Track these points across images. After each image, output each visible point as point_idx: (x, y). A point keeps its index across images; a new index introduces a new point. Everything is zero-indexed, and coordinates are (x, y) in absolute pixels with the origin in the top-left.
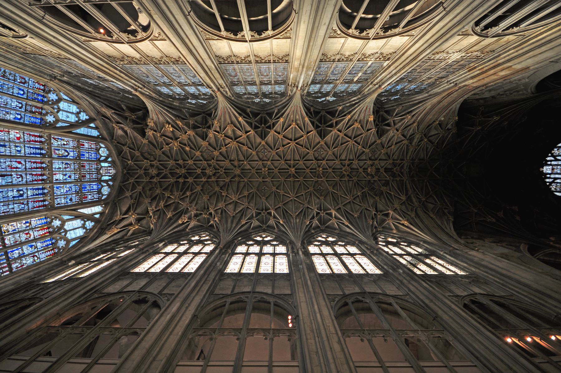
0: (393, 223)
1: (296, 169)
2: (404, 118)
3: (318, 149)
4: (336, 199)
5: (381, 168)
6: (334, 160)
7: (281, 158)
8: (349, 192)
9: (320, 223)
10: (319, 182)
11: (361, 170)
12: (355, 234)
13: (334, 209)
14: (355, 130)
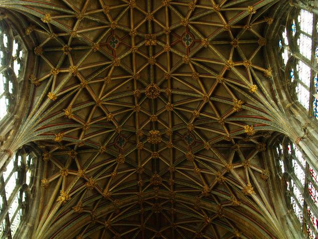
0: (58, 179)
3: (193, 35)
4: (96, 75)
5: (159, 153)
6: (171, 67)
11: (154, 117)
14: (227, 102)
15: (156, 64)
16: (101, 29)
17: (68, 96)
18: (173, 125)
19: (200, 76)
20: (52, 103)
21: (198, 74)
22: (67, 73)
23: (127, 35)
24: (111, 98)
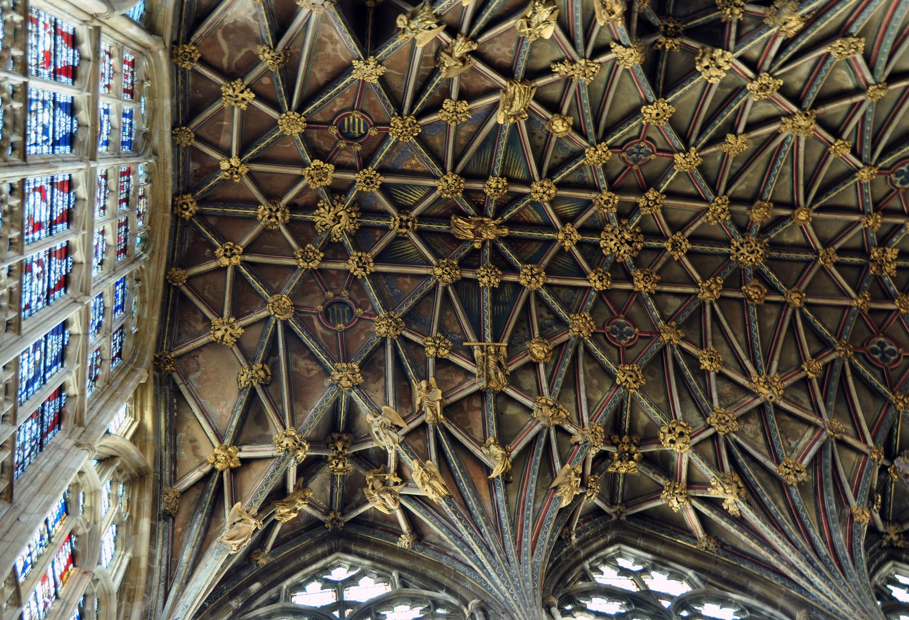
4: (700, 393)
7: (441, 163)
8: (761, 362)
9: (612, 503)
10: (621, 299)
11: (828, 259)
15: (688, 233)
16: (583, 361)
22: (690, 463)
24: (759, 353)
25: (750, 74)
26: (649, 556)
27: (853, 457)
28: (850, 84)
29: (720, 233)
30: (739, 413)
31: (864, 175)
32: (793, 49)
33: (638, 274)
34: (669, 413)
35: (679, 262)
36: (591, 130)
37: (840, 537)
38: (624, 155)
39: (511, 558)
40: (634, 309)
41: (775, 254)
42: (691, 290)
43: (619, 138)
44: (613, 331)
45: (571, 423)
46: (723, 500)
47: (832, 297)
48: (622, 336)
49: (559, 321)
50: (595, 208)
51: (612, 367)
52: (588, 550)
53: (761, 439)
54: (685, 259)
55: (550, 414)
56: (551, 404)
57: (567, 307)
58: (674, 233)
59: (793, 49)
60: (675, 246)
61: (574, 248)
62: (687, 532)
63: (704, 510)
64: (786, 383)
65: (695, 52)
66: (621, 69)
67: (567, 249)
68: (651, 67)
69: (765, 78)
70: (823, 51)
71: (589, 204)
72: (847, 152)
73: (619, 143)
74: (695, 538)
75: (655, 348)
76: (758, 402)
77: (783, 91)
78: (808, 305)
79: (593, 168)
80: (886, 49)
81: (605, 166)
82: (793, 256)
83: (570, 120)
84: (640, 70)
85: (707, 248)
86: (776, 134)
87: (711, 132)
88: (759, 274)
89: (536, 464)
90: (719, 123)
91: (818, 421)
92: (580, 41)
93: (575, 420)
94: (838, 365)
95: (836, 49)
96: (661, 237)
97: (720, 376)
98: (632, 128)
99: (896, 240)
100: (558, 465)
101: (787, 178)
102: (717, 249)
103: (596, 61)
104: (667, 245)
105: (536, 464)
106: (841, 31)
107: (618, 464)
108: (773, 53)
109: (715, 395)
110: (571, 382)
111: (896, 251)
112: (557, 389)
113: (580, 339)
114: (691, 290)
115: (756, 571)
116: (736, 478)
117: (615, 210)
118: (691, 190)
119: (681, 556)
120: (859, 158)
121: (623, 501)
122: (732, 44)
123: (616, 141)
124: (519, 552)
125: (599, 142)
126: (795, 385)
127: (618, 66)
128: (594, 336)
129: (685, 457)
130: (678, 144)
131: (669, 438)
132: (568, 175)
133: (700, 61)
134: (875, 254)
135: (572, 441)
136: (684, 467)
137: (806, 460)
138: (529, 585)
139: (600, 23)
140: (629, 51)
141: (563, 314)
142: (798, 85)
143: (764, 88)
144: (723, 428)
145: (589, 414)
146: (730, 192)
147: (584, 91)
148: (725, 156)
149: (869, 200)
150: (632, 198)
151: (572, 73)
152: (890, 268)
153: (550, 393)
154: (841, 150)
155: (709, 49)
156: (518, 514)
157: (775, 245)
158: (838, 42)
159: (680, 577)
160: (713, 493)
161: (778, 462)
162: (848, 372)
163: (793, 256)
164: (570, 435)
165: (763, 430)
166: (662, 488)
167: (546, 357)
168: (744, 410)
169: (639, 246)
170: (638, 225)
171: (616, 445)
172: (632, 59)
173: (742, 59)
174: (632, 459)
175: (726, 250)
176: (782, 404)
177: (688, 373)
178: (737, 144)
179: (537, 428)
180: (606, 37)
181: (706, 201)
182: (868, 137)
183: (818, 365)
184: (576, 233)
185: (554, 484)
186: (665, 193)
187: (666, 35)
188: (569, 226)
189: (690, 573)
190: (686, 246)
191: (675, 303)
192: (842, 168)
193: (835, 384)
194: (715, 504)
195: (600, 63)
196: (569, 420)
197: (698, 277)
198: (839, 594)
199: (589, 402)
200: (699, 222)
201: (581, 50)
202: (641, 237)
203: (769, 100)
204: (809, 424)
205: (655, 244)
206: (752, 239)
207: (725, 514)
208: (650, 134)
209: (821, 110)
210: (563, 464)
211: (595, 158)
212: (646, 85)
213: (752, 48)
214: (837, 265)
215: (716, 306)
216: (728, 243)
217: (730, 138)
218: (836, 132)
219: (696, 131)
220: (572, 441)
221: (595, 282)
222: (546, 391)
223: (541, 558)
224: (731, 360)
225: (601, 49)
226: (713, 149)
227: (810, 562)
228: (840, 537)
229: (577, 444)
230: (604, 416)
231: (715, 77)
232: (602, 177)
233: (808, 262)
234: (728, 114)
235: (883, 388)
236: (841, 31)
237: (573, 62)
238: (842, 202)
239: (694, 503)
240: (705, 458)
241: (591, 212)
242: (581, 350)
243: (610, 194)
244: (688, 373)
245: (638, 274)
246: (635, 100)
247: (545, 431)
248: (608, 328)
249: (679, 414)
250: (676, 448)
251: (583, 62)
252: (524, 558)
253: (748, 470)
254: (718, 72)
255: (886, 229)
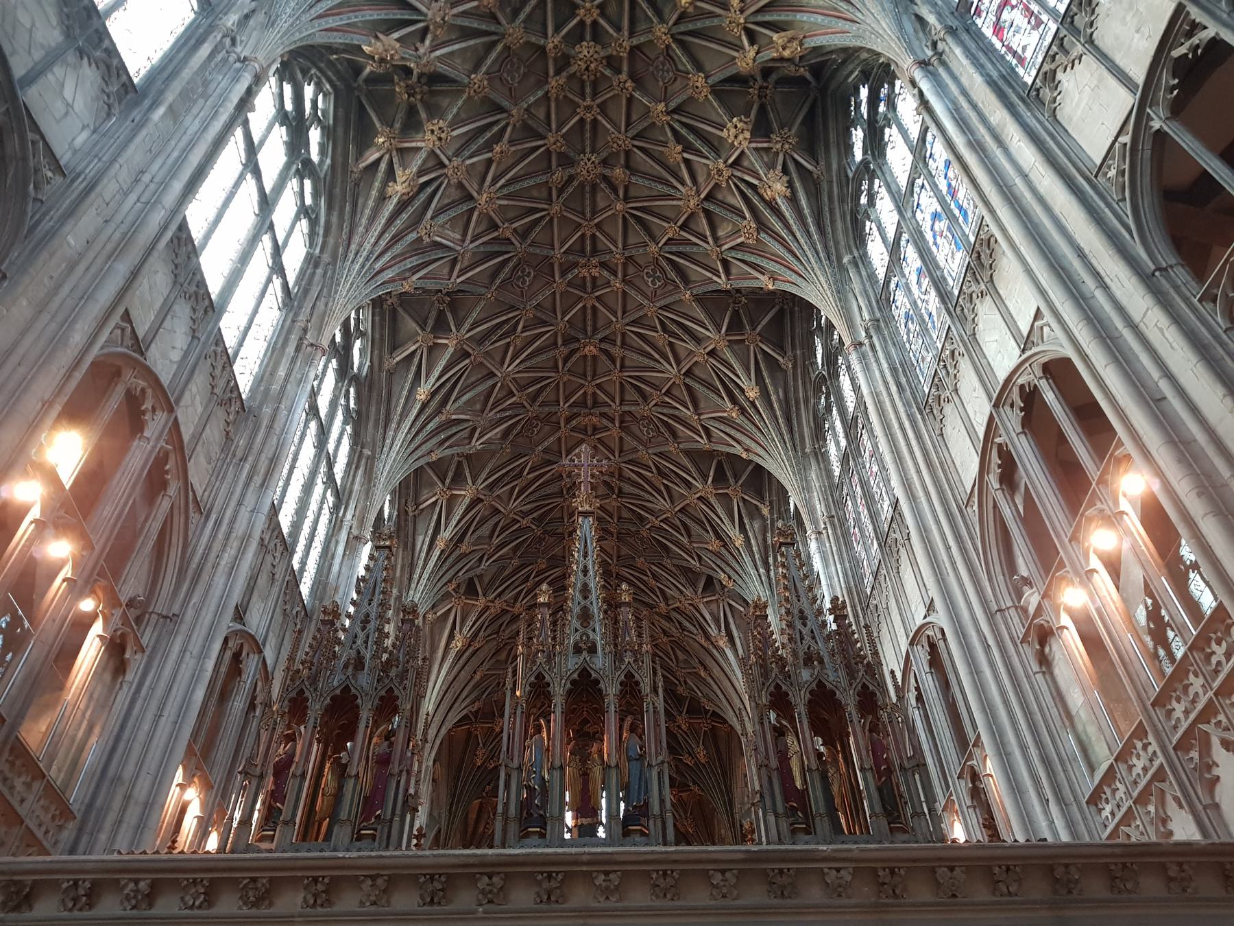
0: (450, 610)
1: (594, 357)
2: (733, 521)
3: (664, 271)
4: (474, 147)
6: (628, 124)
8: (505, 191)
9: (367, 81)
12: (416, 576)
13: (461, 342)
15: (599, 118)
17: (448, 385)
18: (622, 400)
19: (671, 339)
20: (460, 654)
21: (667, 336)
22: (418, 149)
23: (548, 263)
24: (511, 189)
25: (730, 161)
26: (331, 122)
27: (446, 271)
28: (721, 233)
29: (600, 144)
30: (464, 182)
31: (653, 248)
32: (749, 192)
33: (562, 80)
34: (453, 125)
35: (575, 113)
36: (682, 28)
37: (389, 274)
38: (661, 58)
39: (313, 11)
40: (532, 79)
41: (588, 189)
42: (554, 126)
43: (676, 54)
44: (513, 64)
45: (432, 41)
46: (395, 182)
47: (559, 235)
48: (509, 72)
49: (516, 13)
50: (615, 35)
51: (484, 69)
52: (325, 69)
53: (446, 201)
54: (577, 118)
55: (438, 19)
56: (446, 19)
57: (529, 16)
58: (598, 106)
59: (749, 192)
60: (588, 108)
61: (578, 18)
62: (360, 154)
63: (383, 166)
64: (492, 213)
65: (748, 116)
66: (735, 54)
67: (577, 12)
68: (739, 80)
69: (726, 174)
70: (747, 215)
71: (618, 29)
72: (670, 235)
73: (671, 53)
74: (357, 160)
75: (505, 104)
76: (475, 194)
77: (717, 186)
78: (551, 220)
79: (650, 30)
80: (746, 257)
81: (651, 41)
82: (588, 202)
83: (691, 10)
84: (734, 72)
85: (588, 135)
86: (683, 183)
87: (683, 131)
88: (571, 178)
89: (394, 14)
90: (691, 138)
91: (468, 242)
92: (760, 18)
93: (436, 43)
94: (510, 248)
95: (749, 222)
96: (594, 95)
97: (490, 162)
98: (685, 65)
99: (605, 273)
100: (396, 35)
101: (647, 193)
102: (588, 142)
103: (743, 32)
104: (588, 102)
105: (394, 14)
106: (762, 226)
107: (402, 84)
108: (747, 178)
109: (475, 160)
110: (466, 33)
111: (597, 275)
112: (459, 22)
113: (503, 36)
114: (554, 126)
115: (347, 216)
116: (415, 190)
117: (615, 53)
118: (634, 117)
119: (339, 150)
120: (665, 244)
121: (370, 91)
122: (754, 145)
123: (674, 50)
124: (320, 17)
125: (672, 36)
126: (491, 219)
127: (738, 51)
128: (507, 48)
129: (423, 144)
130: (673, 105)
131: (435, 128)
132: (642, 8)
133: (741, 121)
134: (594, 261)
135: (418, 45)
136: (414, 145)
137: (438, 239)
138: (298, 36)
139: (775, 37)
140: (750, 62)
141: (522, 16)
142: (720, 197)
143: (720, 172)
144: (451, 171)
145: (442, 55)
146: (635, 150)
147: (716, 21)
148: (664, 144)
149: (633, 252)
150: (625, 68)
151: (732, 11)
152: (584, 272)
153: (454, 15)
154: (672, 231)
155: (750, 127)
156: (349, 7)
157: (594, 187)
158: (754, 225)
159: (322, 152)
160: (399, 172)
161: (432, 218)
162: (506, 256)
163: (588, 202)
164: (423, 41)
165: (453, 202)
166: (391, 127)
167: (485, 7)
168: (467, 185)
169: (585, 77)
170: (602, 74)
171: (419, 81)
172: (744, 65)
173: (743, 153)
174: (409, 97)
175: (588, 150)
176: (476, 214)
177: (488, 135)
178: (675, 152)
179: (423, 9)
180: (763, 41)
181: (626, 131)
182: (681, 249)
183: (508, 234)
184: (592, 19)
185: (380, 36)
186: (631, 95)
187: (761, 88)
188: (598, 11)
189: (328, 161)
190: (589, 117)
191: (541, 113)
192: (657, 233)
193: (496, 248)
194: (391, 175)
195: (740, 35)
196: (435, 37)
197: (564, 131)
198: (352, 285)
199: (452, 53)
200: (609, 126)
201: (752, 19)
202: (592, 77)
203: (709, 174)
204: (464, 234)
205: (588, 90)
206: (599, 170)
207: (385, 184)
208: (679, 79)
209: (702, 215)
210: (398, 40)
211: (659, 34)
212: (721, 76)
213: (753, 160)
214: (583, 235)
215: (542, 149)
216: (592, 152)
217: (679, 148)
218: (684, 227)
219: (684, 120)
220: (418, 45)
221: (553, 42)
222: (455, 11)
223: (320, 39)
224: (503, 167)
225: (752, 37)
226: (669, 134)
227: (367, 259)
228: (389, 274)
229: (417, 49)
230: (442, 68)
231: (728, 134)
232: (642, 39)
233: (583, 214)
234: (698, 144)
235: (498, 281)
236: (762, 226)
237: (742, 11)
238: (630, 233)
239: (387, 156)
240: (425, 161)
241: (611, 31)
242: (495, 38)
243: (628, 48)
244: (488, 135)
245: (562, 80)
246: (708, 66)
247: (422, 18)
248: (515, 60)
249: (455, 133)
250: (428, 136)
251: (742, 21)
252: (316, 22)
253: (423, 197)
254: (732, 138)
255: (612, 266)
